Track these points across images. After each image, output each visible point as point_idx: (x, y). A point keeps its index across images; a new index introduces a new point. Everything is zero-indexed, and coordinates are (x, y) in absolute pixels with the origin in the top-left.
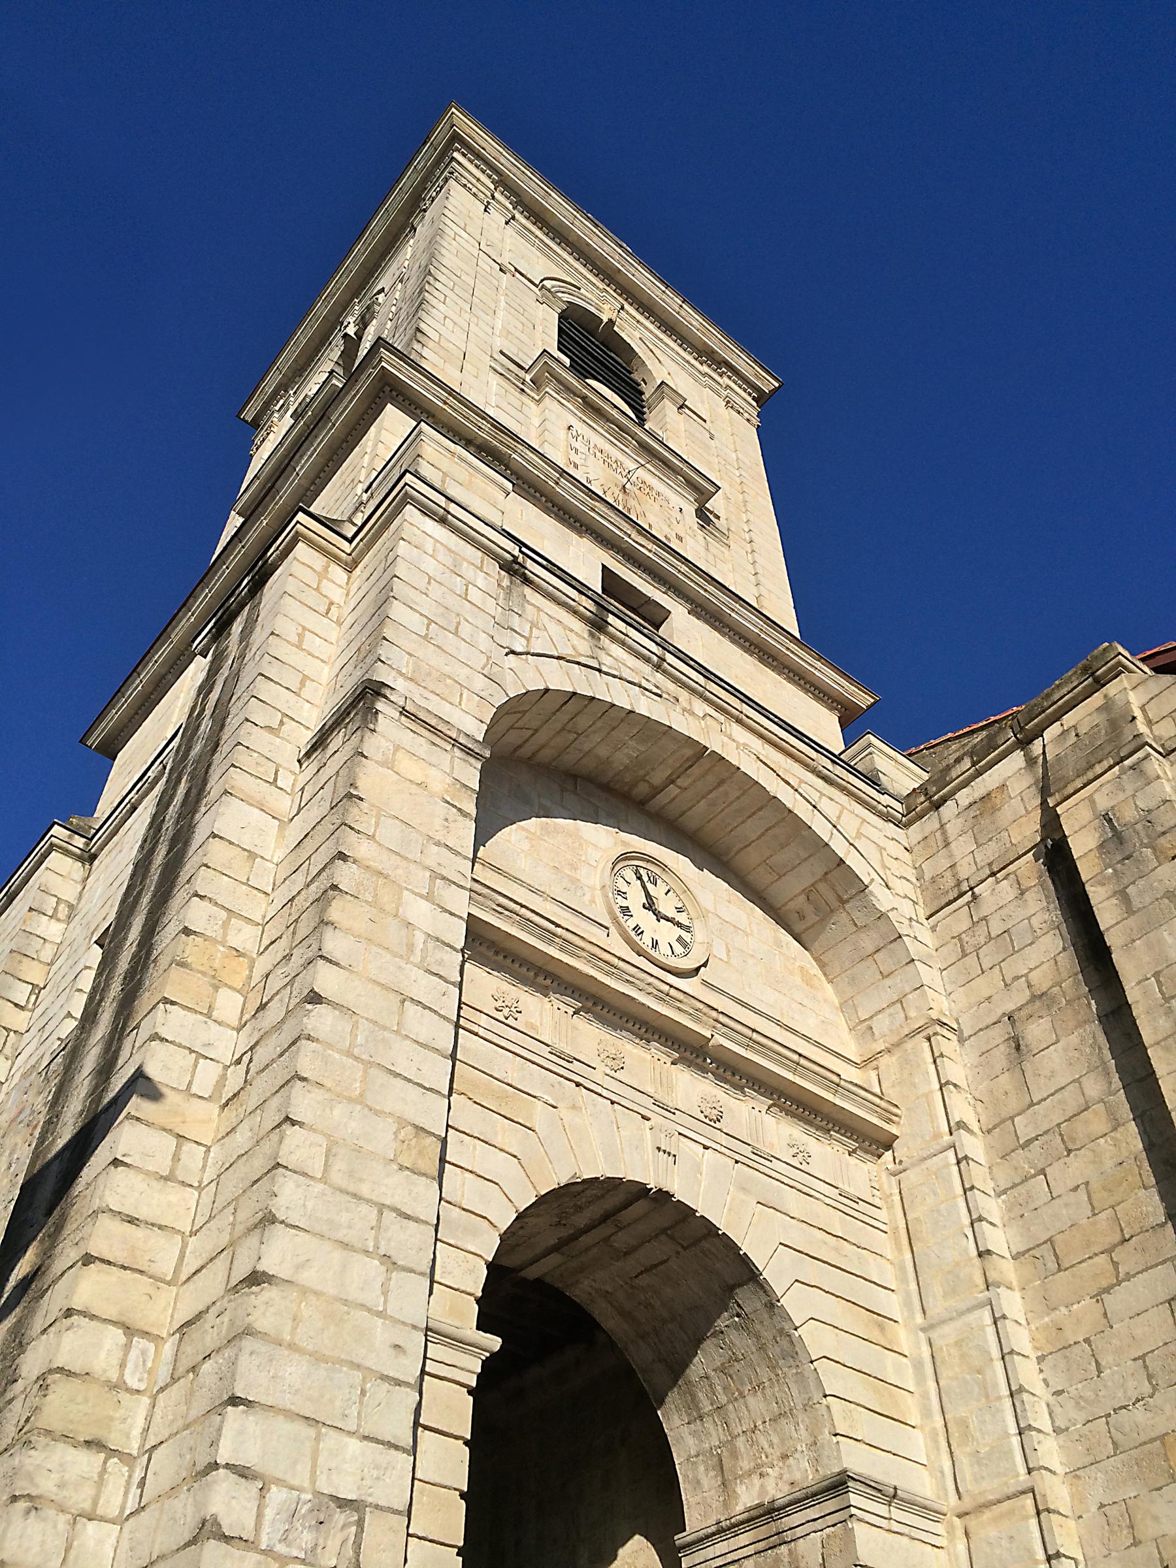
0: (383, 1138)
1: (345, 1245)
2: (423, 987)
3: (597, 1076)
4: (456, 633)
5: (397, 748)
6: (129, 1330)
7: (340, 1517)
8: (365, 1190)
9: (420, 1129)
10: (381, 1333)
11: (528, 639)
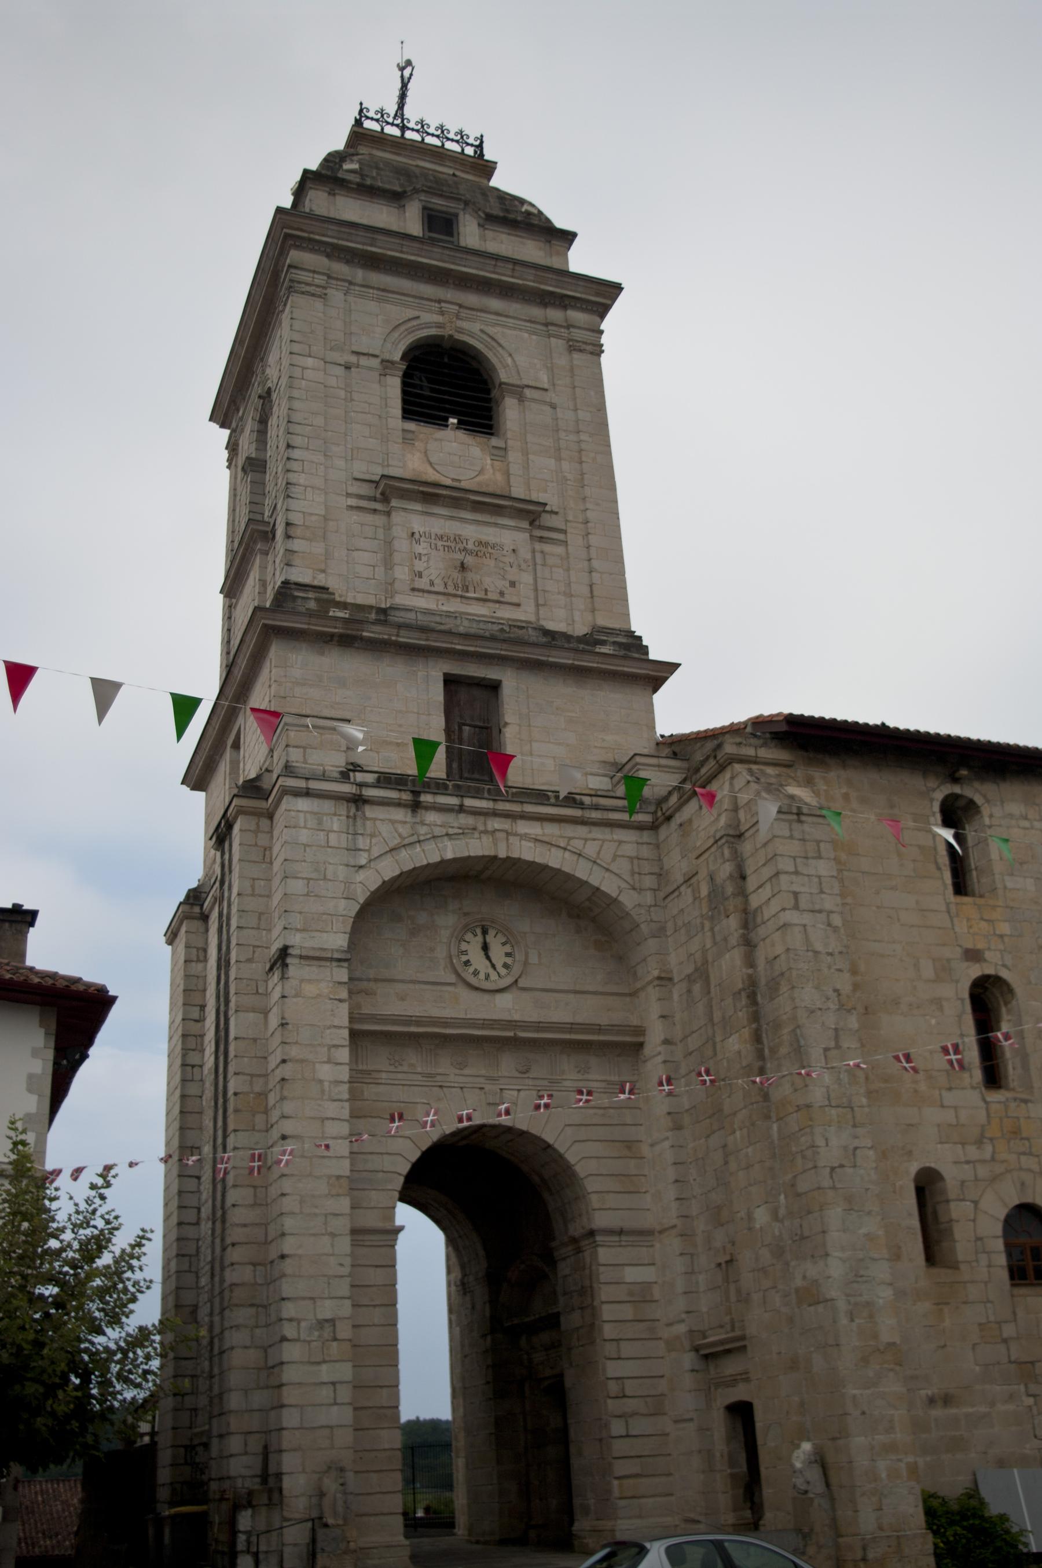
1: (314, 1235)
2: (332, 1109)
3: (452, 1078)
4: (325, 879)
5: (302, 981)
6: (254, 1265)
7: (327, 1325)
9: (338, 1177)
11: (368, 851)
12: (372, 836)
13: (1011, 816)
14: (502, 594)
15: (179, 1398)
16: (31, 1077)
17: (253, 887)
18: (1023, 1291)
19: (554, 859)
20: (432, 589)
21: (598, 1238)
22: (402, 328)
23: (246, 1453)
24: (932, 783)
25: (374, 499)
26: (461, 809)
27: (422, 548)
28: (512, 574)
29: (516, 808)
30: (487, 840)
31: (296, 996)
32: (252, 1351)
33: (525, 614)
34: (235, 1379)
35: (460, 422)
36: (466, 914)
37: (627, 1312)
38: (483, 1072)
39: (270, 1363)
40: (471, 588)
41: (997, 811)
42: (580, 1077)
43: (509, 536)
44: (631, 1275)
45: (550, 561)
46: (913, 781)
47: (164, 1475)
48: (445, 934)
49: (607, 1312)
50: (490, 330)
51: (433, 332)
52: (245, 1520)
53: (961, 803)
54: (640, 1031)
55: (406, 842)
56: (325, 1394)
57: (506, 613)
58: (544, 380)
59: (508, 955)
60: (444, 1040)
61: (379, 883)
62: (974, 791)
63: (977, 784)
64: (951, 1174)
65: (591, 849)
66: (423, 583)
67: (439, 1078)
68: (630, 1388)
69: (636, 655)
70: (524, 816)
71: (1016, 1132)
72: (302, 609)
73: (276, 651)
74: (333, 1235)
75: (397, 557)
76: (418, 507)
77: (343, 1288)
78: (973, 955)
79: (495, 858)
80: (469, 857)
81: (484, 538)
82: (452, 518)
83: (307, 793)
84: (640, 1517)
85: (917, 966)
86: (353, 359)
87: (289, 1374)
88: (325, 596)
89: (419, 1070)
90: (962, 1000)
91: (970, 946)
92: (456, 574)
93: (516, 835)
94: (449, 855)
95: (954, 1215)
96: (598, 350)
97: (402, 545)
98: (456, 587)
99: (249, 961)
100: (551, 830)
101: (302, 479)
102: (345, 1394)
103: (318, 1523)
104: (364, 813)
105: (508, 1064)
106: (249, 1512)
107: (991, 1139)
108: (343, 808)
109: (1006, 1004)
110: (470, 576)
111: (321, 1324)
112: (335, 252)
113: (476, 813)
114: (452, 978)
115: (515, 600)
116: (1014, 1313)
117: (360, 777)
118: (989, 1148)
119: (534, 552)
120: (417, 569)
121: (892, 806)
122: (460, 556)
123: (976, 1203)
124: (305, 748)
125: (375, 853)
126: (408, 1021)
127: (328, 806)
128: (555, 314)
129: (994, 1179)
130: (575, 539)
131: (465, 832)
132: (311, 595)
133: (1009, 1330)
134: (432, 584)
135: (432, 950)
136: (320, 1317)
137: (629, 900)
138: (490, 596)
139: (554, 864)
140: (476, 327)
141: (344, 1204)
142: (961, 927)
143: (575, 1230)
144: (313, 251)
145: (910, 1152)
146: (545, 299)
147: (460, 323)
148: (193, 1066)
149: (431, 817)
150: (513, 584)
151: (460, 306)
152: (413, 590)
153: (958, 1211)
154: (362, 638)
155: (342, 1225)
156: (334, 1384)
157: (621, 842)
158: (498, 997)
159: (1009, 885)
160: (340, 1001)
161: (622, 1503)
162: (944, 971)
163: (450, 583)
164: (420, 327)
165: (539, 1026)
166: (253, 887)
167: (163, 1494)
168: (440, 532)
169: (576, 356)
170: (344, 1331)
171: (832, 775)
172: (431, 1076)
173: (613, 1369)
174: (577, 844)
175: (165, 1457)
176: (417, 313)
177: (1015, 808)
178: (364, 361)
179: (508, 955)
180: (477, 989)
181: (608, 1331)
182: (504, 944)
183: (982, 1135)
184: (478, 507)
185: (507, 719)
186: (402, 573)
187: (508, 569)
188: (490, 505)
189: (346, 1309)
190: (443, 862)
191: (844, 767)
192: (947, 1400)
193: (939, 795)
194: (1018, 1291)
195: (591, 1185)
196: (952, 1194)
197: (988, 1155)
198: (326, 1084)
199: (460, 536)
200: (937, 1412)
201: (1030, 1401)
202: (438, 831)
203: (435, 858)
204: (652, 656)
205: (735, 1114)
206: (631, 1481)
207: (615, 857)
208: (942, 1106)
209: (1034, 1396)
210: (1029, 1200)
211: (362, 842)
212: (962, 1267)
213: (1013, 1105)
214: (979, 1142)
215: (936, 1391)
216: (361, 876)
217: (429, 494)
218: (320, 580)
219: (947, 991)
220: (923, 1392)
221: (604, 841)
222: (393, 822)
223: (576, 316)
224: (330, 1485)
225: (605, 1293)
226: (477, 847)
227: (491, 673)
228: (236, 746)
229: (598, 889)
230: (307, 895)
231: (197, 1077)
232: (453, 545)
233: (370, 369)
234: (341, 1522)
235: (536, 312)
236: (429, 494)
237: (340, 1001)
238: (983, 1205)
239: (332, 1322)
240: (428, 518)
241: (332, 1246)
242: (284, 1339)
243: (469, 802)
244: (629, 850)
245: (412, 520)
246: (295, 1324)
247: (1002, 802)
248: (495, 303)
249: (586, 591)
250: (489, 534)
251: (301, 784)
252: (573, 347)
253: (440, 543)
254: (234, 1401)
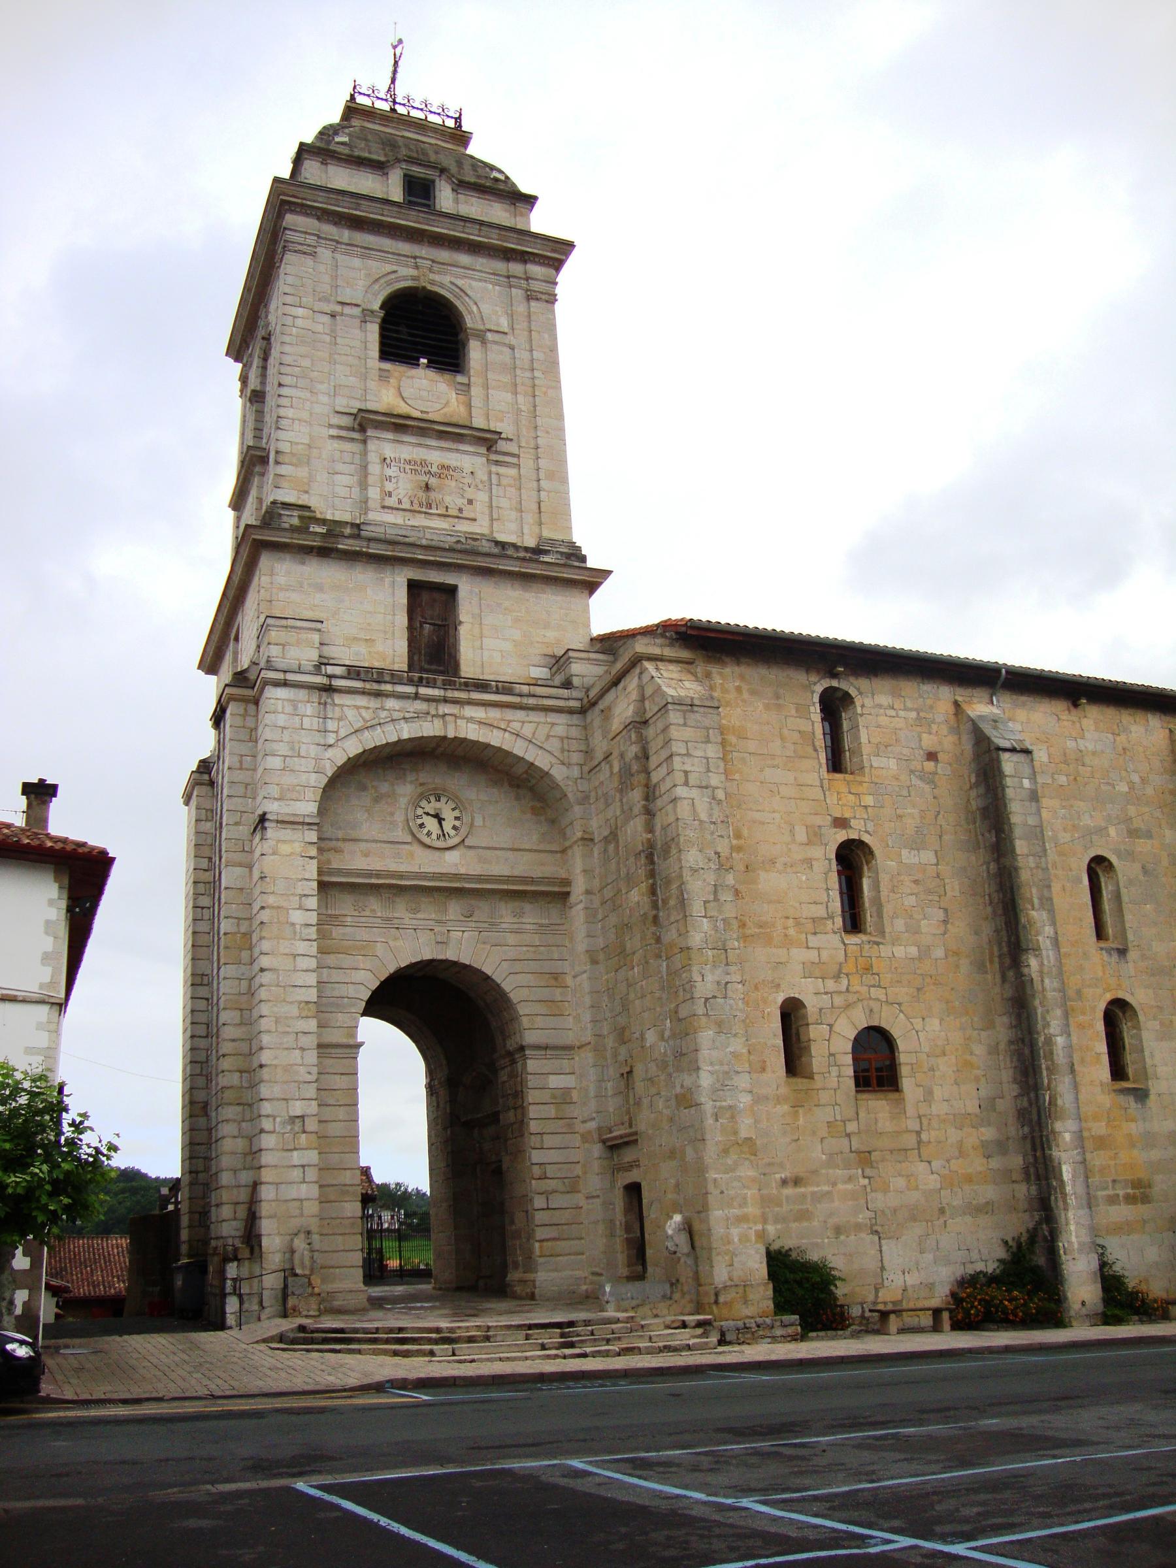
0: (294, 1011)
2: (301, 947)
4: (299, 756)
5: (278, 841)
6: (241, 1072)
7: (297, 1120)
8: (289, 1030)
9: (307, 1003)
10: (302, 1070)
12: (340, 719)
13: (880, 706)
14: (461, 510)
15: (194, 1175)
16: (48, 922)
17: (241, 762)
18: (865, 1096)
19: (495, 739)
21: (527, 1052)
22: (382, 281)
23: (235, 1219)
24: (813, 678)
25: (353, 429)
26: (417, 696)
27: (389, 472)
28: (470, 493)
29: (463, 695)
30: (438, 723)
31: (274, 854)
32: (239, 1140)
33: (480, 527)
34: (226, 1161)
35: (429, 361)
36: (421, 785)
37: (551, 1111)
38: (433, 916)
39: (255, 1149)
40: (434, 506)
41: (868, 702)
42: (515, 920)
43: (468, 460)
44: (554, 1081)
45: (504, 481)
46: (800, 677)
47: (184, 1235)
48: (403, 801)
49: (533, 1111)
50: (460, 282)
51: (409, 283)
52: (232, 1270)
53: (839, 694)
54: (567, 882)
55: (369, 724)
56: (296, 1174)
57: (464, 527)
58: (504, 324)
59: (457, 818)
60: (402, 889)
61: (345, 759)
62: (850, 685)
63: (852, 679)
64: (812, 1004)
65: (527, 730)
67: (396, 921)
68: (550, 1171)
69: (577, 564)
70: (470, 702)
71: (868, 969)
72: (287, 526)
73: (266, 561)
74: (302, 1049)
75: (371, 480)
76: (390, 436)
77: (311, 1092)
78: (841, 823)
79: (445, 738)
80: (423, 737)
81: (447, 462)
83: (285, 684)
84: (556, 1270)
85: (792, 832)
86: (338, 308)
87: (266, 1159)
88: (307, 514)
89: (379, 914)
90: (830, 860)
91: (839, 816)
92: (421, 494)
93: (463, 718)
94: (405, 736)
95: (812, 1036)
96: (552, 299)
97: (374, 468)
98: (421, 505)
99: (237, 824)
100: (494, 714)
101: (290, 413)
102: (312, 1174)
103: (289, 1273)
104: (333, 700)
105: (454, 909)
106: (235, 1263)
107: (847, 975)
108: (315, 696)
109: (867, 863)
110: (433, 495)
111: (293, 1119)
112: (325, 215)
113: (428, 700)
114: (409, 839)
115: (472, 516)
116: (857, 1114)
117: (330, 670)
118: (845, 982)
119: (490, 473)
121: (778, 698)
123: (831, 1026)
124: (284, 645)
125: (342, 733)
126: (370, 874)
127: (302, 694)
128: (516, 268)
129: (848, 1006)
130: (527, 462)
131: (419, 716)
132: (296, 513)
133: (852, 1127)
134: (400, 502)
135: (392, 814)
136: (292, 1114)
137: (558, 773)
138: (451, 512)
139: (495, 742)
140: (446, 279)
141: (312, 1025)
142: (832, 799)
143: (511, 1045)
144: (307, 215)
145: (778, 985)
146: (508, 255)
147: (432, 276)
148: (203, 908)
149: (391, 703)
150: (470, 502)
151: (433, 261)
152: (384, 507)
153: (815, 1032)
154: (337, 550)
155: (311, 1041)
156: (303, 1166)
157: (553, 724)
158: (447, 853)
159: (875, 764)
160: (311, 858)
161: (541, 1260)
162: (814, 836)
163: (416, 501)
164: (398, 280)
165: (479, 878)
166: (241, 762)
167: (184, 1248)
168: (408, 458)
169: (533, 303)
170: (311, 1125)
171: (728, 670)
172: (389, 919)
173: (536, 1156)
174: (516, 726)
175: (185, 1220)
176: (395, 268)
177: (884, 699)
178: (348, 310)
179: (457, 818)
180: (430, 847)
181: (534, 1126)
182: (453, 810)
183: (840, 972)
184: (442, 435)
185: (462, 618)
186: (374, 493)
188: (452, 433)
189: (313, 1108)
190: (399, 741)
191: (738, 664)
192: (797, 1182)
193: (819, 689)
194: (860, 1096)
195: (522, 1010)
196: (810, 1020)
197: (844, 988)
198: (298, 927)
200: (789, 1191)
201: (866, 1181)
202: (396, 715)
203: (393, 738)
204: (590, 564)
205: (634, 953)
206: (549, 1244)
207: (548, 736)
208: (808, 948)
209: (869, 1178)
210: (876, 1024)
211: (331, 725)
212: (816, 1077)
213: (867, 947)
214: (837, 977)
215: (789, 1175)
216: (330, 753)
217: (399, 425)
218: (303, 500)
219: (817, 852)
220: (778, 1176)
221: (538, 723)
222: (358, 708)
223: (535, 270)
224: (300, 1243)
225: (532, 1096)
226: (430, 729)
227: (449, 579)
228: (237, 639)
229: (532, 764)
230: (284, 769)
231: (206, 917)
232: (419, 468)
233: (352, 316)
234: (307, 1272)
235: (500, 266)
236: (399, 425)
237: (311, 858)
238: (837, 1028)
239: (303, 1117)
241: (302, 1058)
242: (262, 1131)
243: (423, 691)
244: (560, 730)
245: (384, 446)
246: (271, 1119)
247: (873, 695)
248: (464, 259)
249: (535, 507)
250: (452, 459)
251: (280, 676)
252: (530, 297)
253: (408, 467)
254: (225, 1178)
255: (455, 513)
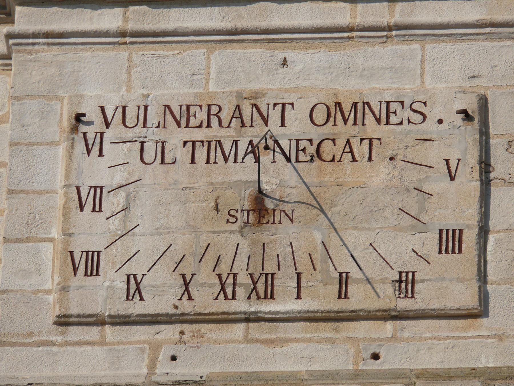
14: (405, 283)
20: (137, 308)
40: (285, 283)
66: (103, 293)
81: (350, 88)
82: (235, 35)
92: (233, 244)
98: (226, 288)
110: (284, 237)
120: (80, 245)
122: (245, 171)
134: (134, 288)
138: (359, 298)
150: (450, 241)
187: (438, 184)
199: (257, 95)
240: (142, 55)
253: (176, 137)
255: (387, 298)
